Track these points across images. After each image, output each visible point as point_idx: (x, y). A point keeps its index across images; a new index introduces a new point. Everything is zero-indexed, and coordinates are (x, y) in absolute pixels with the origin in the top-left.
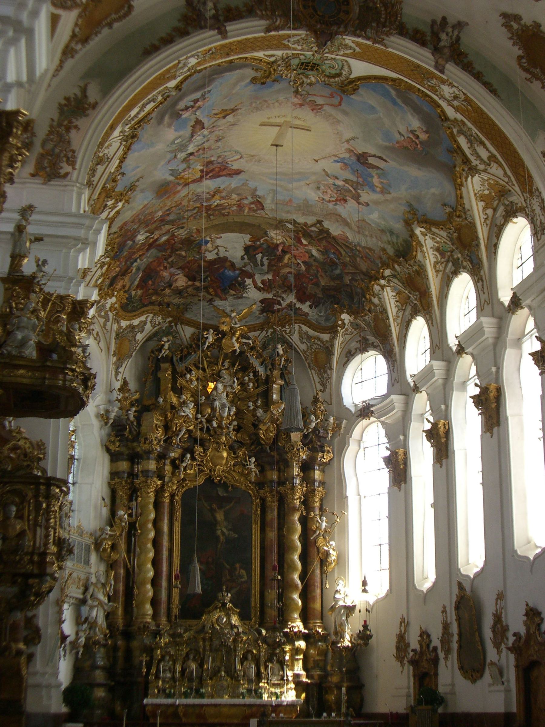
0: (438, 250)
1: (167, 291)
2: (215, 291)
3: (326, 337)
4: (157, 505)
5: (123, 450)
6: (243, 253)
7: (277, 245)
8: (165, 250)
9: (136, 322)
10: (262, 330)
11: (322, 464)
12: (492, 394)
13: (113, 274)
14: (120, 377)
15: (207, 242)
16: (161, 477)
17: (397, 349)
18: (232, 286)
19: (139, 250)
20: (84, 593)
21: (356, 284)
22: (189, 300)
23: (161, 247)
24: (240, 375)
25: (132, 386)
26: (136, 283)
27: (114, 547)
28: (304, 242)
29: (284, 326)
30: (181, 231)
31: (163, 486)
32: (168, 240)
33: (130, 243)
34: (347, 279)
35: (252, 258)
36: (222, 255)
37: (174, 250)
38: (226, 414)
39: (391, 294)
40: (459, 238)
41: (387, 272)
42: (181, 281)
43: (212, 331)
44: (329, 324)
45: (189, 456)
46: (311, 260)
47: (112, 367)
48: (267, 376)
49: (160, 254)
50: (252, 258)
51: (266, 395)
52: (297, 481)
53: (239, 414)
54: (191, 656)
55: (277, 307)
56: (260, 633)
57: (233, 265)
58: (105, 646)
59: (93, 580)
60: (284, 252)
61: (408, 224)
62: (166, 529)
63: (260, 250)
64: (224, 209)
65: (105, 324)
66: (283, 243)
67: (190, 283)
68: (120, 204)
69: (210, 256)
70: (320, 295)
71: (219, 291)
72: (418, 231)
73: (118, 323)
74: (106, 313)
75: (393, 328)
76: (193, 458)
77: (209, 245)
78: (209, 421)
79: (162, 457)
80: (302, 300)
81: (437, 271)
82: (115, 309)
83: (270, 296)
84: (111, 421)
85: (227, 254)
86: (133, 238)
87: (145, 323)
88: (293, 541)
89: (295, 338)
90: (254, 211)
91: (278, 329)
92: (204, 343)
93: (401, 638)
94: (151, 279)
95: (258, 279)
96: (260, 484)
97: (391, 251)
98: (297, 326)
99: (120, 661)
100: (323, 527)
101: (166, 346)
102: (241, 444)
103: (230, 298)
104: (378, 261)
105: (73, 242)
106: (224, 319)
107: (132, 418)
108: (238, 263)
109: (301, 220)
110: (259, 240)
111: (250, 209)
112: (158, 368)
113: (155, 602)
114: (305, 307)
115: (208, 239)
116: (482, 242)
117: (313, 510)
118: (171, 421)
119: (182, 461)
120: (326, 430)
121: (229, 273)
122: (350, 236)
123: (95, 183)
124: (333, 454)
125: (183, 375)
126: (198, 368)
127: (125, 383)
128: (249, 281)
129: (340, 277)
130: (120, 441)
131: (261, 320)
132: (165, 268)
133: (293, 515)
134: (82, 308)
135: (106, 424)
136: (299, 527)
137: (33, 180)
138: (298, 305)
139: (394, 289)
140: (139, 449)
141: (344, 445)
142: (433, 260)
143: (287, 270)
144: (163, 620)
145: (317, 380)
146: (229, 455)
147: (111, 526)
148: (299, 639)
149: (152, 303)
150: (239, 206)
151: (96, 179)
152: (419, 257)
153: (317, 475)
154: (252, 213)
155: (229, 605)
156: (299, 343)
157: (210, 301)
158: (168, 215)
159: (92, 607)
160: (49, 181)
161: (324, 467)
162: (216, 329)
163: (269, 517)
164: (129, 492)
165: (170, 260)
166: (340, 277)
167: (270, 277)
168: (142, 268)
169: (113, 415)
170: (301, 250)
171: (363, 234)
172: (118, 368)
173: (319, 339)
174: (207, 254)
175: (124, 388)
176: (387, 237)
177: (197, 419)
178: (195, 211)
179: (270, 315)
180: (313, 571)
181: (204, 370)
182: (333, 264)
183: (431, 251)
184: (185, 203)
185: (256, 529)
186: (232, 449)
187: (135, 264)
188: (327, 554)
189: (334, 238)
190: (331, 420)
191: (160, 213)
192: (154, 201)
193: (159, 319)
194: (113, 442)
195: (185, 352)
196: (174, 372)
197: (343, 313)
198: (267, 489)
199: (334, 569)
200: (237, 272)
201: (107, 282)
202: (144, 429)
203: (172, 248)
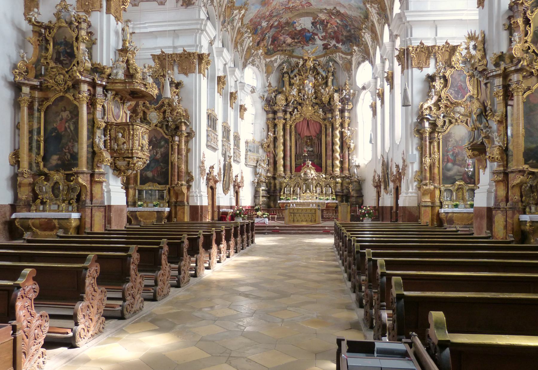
0: (378, 14)
1: (284, 45)
2: (304, 43)
3: (349, 57)
4: (284, 129)
5: (270, 109)
6: (311, 25)
7: (324, 20)
8: (279, 28)
9: (273, 59)
10: (325, 57)
11: (348, 110)
12: (390, 75)
13: (257, 41)
14: (269, 81)
15: (295, 23)
16: (285, 119)
17: (373, 60)
18: (310, 40)
19: (266, 29)
20: (256, 164)
21: (356, 33)
22: (294, 47)
23: (276, 27)
24: (316, 76)
25: (274, 84)
26: (270, 43)
27: (268, 146)
28: (333, 17)
29: (333, 54)
30: (282, 19)
31: (286, 122)
32: (278, 24)
33: (259, 27)
34: (352, 31)
35: (316, 27)
36: (303, 27)
37: (283, 28)
38: (310, 92)
39: (368, 36)
40: (381, 7)
41: (364, 26)
42: (289, 40)
43: (301, 59)
44: (349, 52)
45: (296, 110)
46: (338, 25)
47: (265, 78)
48: (326, 76)
49: (277, 30)
50: (316, 27)
51: (326, 84)
52: (338, 117)
53: (315, 92)
54: (297, 185)
55: (329, 47)
56: (322, 176)
57: (309, 31)
58: (265, 182)
59: (260, 159)
60: (327, 23)
61: (364, 4)
62: (288, 138)
63: (318, 23)
64: (296, 7)
65: (260, 61)
66: (325, 19)
67: (293, 40)
68: (243, 12)
69: (299, 28)
70: (345, 40)
71: (305, 43)
72: (368, 6)
73: (265, 60)
74: (260, 56)
75: (371, 51)
76: (298, 111)
77: (297, 24)
78: (304, 96)
79: (285, 112)
80: (338, 42)
81: (379, 23)
82: (263, 55)
83: (326, 42)
84: (265, 99)
85: (306, 27)
86: (260, 25)
87: (277, 59)
88: (336, 141)
89: (338, 59)
90: (309, 6)
91: (331, 56)
92: (299, 65)
93: (374, 177)
94: (276, 40)
95: (320, 35)
96: (324, 119)
97: (362, 17)
98: (337, 54)
99: (272, 188)
100: (348, 135)
101: (285, 68)
102: (317, 104)
103: (310, 45)
104: (360, 22)
105: (197, 31)
106: (305, 54)
107: (273, 97)
108: (311, 30)
109: (328, 8)
110: (316, 19)
111: (306, 6)
112: (283, 76)
113: (284, 166)
114: (339, 45)
115: (295, 21)
116: (388, 7)
117: (344, 128)
118: (288, 97)
119: (293, 112)
120: (350, 96)
121: (308, 34)
122: (347, 12)
123: (222, 4)
124: (353, 105)
125: (293, 79)
126: (299, 75)
127: (270, 84)
128: (316, 37)
129: (350, 31)
130: (269, 106)
131: (324, 53)
132: (281, 35)
133: (336, 131)
134: (202, 57)
135: (263, 100)
136: (338, 135)
137: (182, 8)
138: (337, 45)
139: (369, 34)
140: (275, 109)
141: (357, 101)
142: (377, 19)
143: (330, 30)
144: (288, 172)
145: (347, 75)
146: (311, 109)
147: (267, 139)
148: (338, 178)
149: (278, 51)
150: (302, 5)
151: (222, 3)
152: (372, 18)
153: (346, 114)
154: (308, 8)
155: (310, 166)
156: (339, 61)
157: (303, 47)
158: (273, 13)
159: (260, 169)
160: (187, 7)
161: (349, 111)
162: (303, 58)
163: (328, 132)
164: (273, 125)
165: (282, 32)
166: (350, 31)
167: (324, 34)
168: (271, 37)
169: (265, 97)
170: (333, 21)
171: (351, 10)
172: (267, 78)
173: (346, 58)
174: (297, 28)
175: (270, 85)
176: (359, 11)
177: (299, 95)
178: (284, 10)
179: (327, 50)
180: (345, 152)
181: (302, 75)
182: (346, 26)
183: (375, 15)
184: (277, 7)
185: (323, 137)
186: (312, 106)
187: (267, 35)
188: (350, 146)
189: (342, 14)
190: (352, 91)
191: (268, 13)
192: (261, 8)
193: (283, 57)
194: (266, 107)
195: (293, 69)
196: (290, 77)
197: (353, 46)
198: (327, 121)
199: (353, 151)
200: (311, 34)
201: (256, 44)
202: (277, 101)
203: (282, 27)
